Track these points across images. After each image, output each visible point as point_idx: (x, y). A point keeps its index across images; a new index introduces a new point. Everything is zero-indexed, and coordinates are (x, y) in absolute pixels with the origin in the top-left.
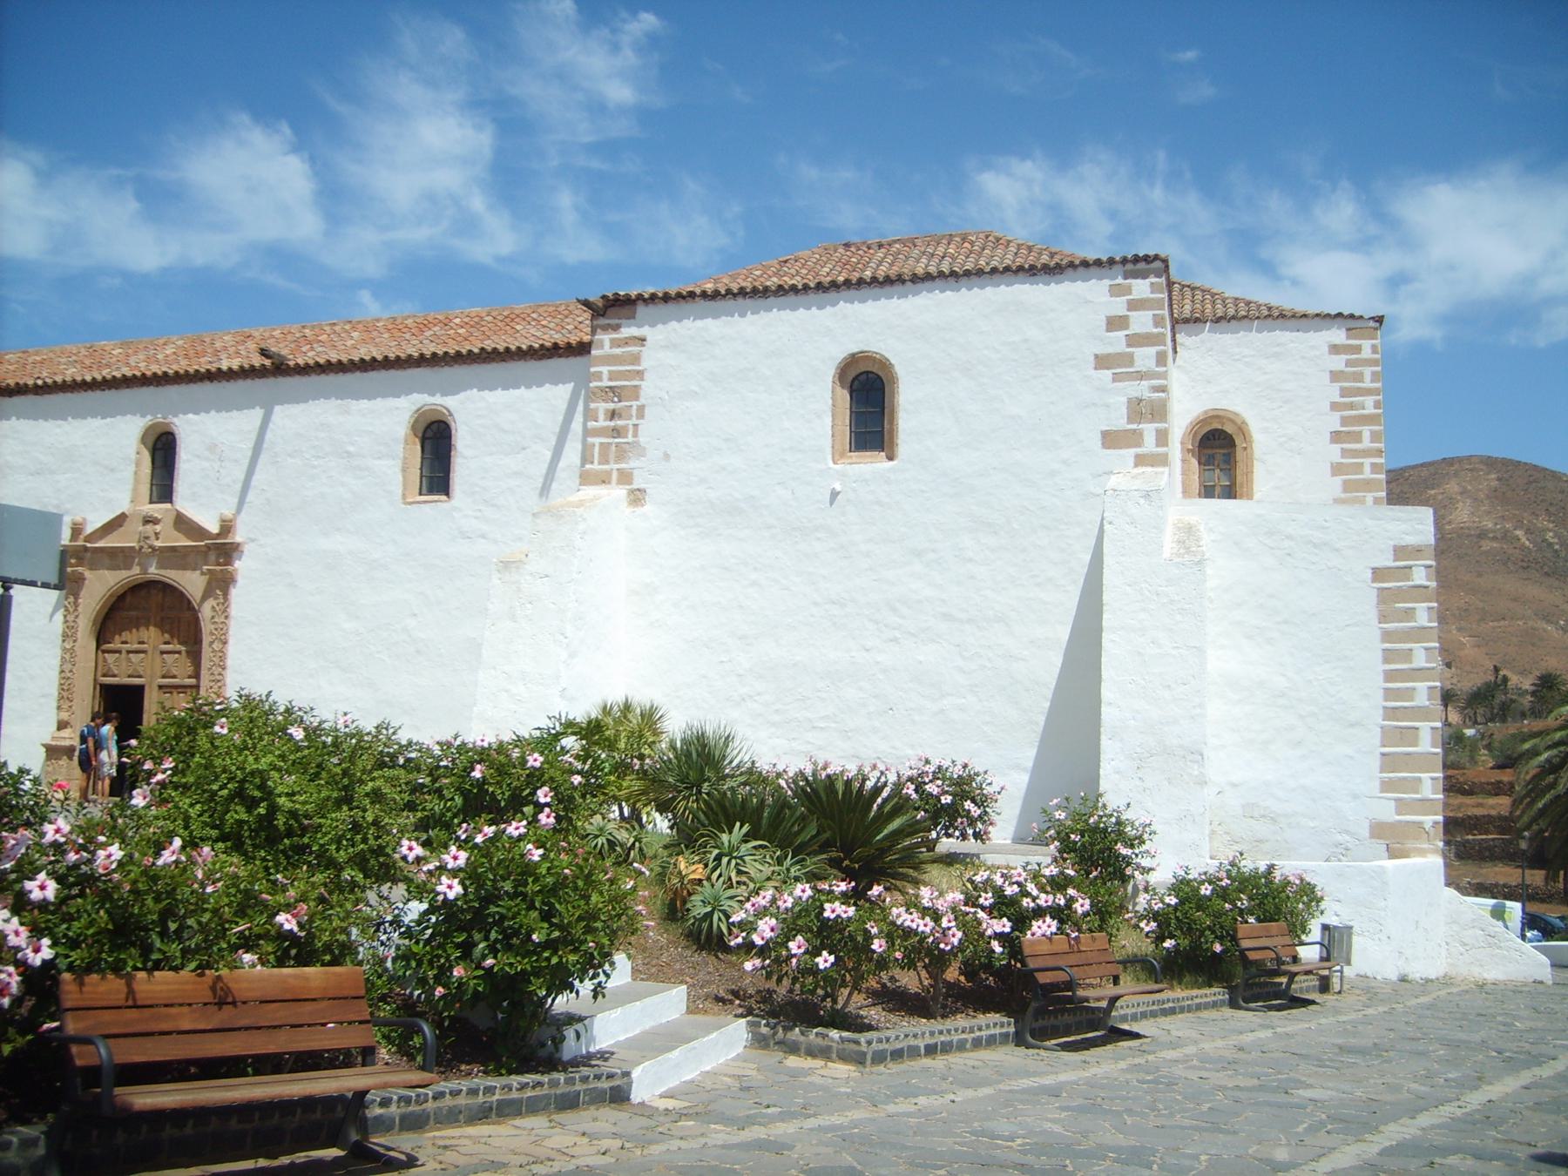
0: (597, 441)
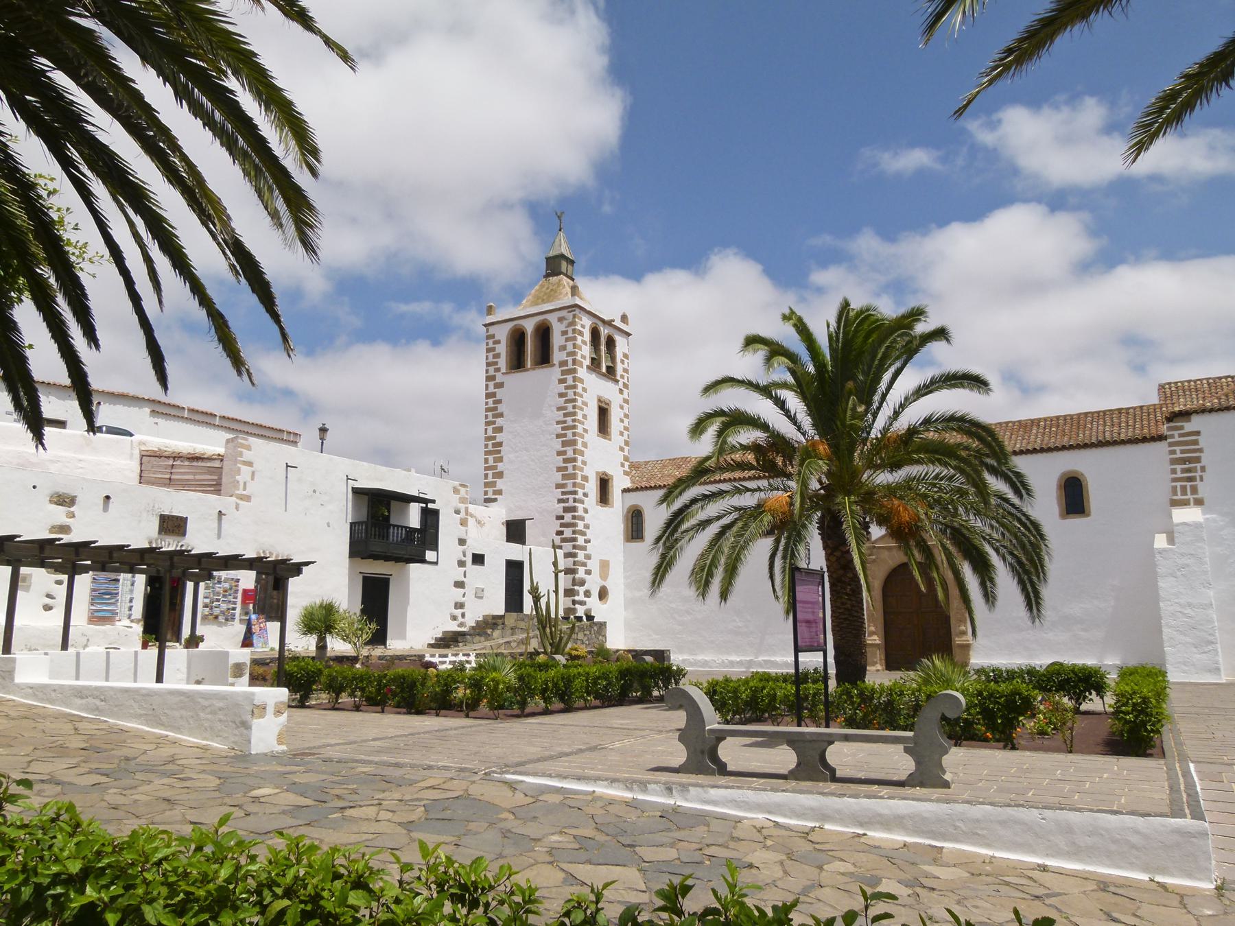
0: (1178, 484)
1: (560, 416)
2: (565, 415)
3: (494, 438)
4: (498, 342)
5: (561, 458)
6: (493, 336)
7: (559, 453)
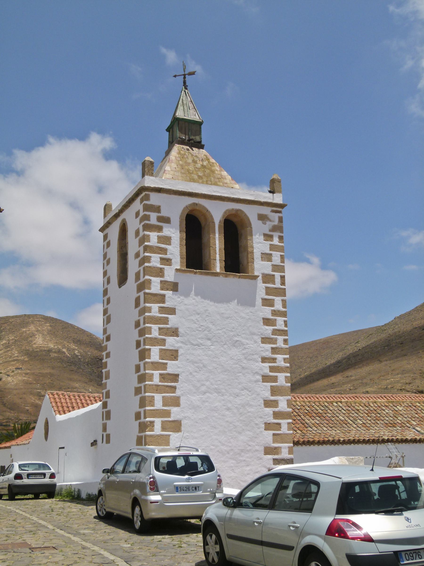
1: (267, 350)
2: (274, 350)
3: (164, 366)
4: (167, 220)
5: (270, 411)
6: (157, 209)
7: (268, 404)
